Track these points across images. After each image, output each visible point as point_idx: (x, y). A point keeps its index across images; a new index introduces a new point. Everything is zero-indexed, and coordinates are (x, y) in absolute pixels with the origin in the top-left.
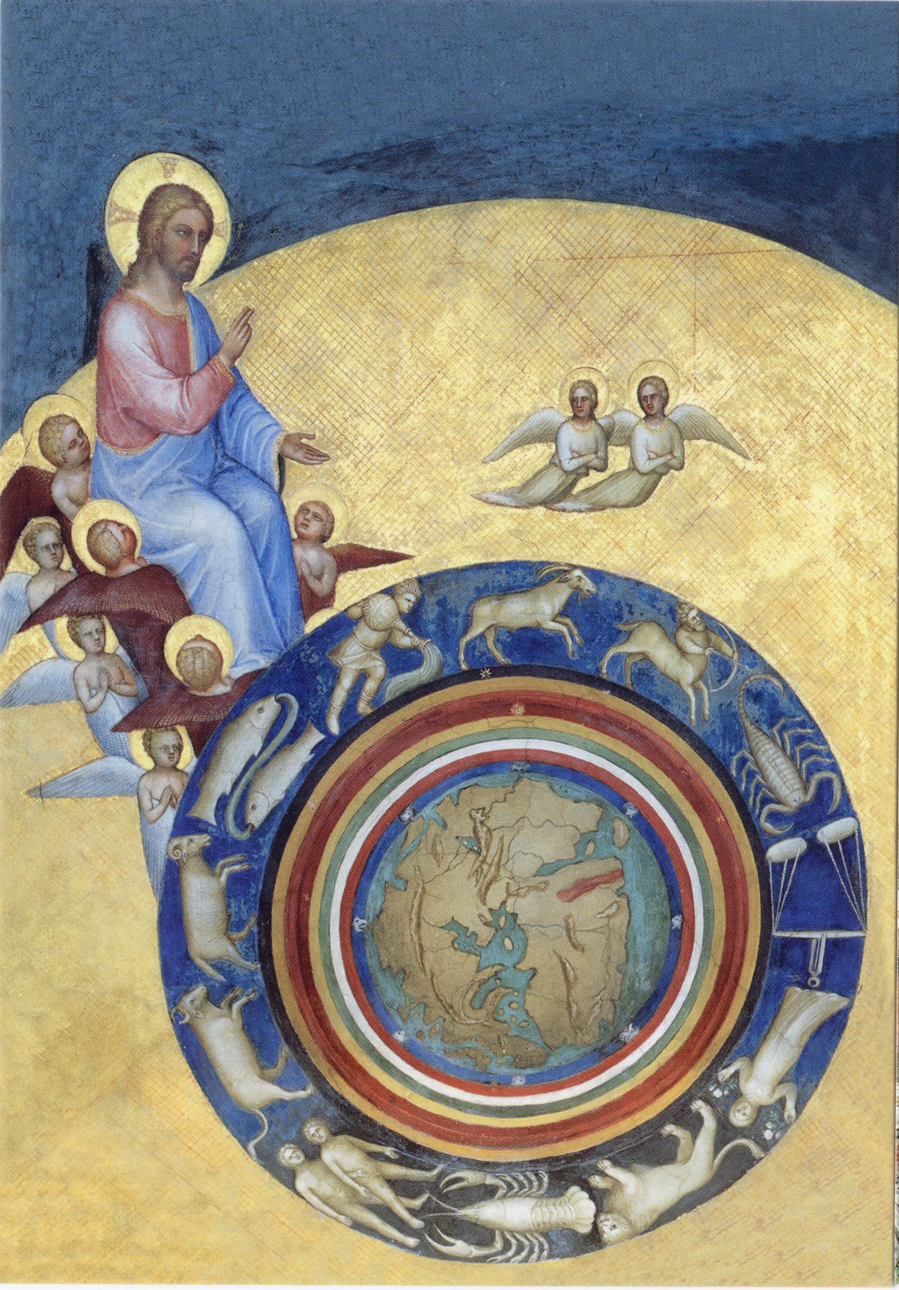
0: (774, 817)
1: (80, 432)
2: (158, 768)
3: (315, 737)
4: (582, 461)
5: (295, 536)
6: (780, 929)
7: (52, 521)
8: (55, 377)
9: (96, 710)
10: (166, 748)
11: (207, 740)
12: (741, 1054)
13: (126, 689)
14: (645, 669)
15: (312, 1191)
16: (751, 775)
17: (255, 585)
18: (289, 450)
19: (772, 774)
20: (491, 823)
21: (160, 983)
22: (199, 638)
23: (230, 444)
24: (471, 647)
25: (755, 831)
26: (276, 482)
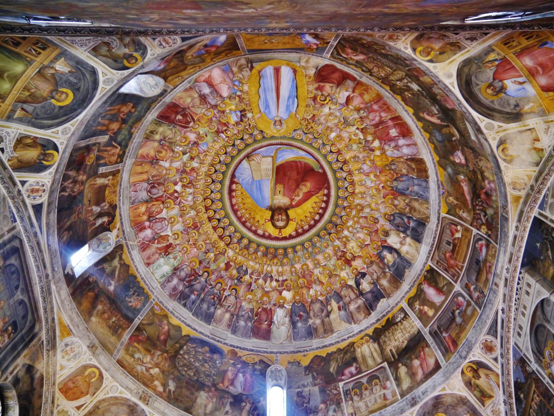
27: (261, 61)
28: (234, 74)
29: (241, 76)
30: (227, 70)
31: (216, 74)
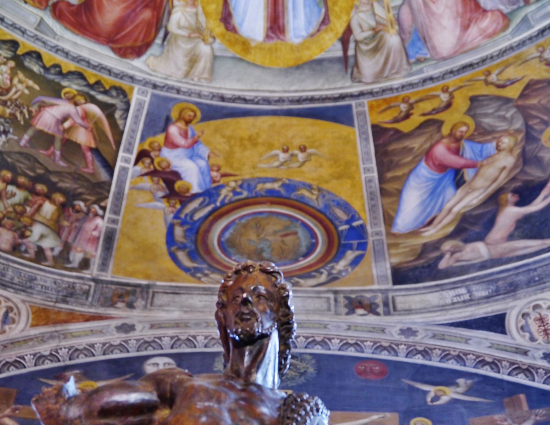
6: (344, 240)
8: (155, 134)
11: (184, 204)
14: (303, 197)
27: (320, 62)
28: (398, 21)
29: (379, 10)
30: (417, 39)
31: (445, 34)
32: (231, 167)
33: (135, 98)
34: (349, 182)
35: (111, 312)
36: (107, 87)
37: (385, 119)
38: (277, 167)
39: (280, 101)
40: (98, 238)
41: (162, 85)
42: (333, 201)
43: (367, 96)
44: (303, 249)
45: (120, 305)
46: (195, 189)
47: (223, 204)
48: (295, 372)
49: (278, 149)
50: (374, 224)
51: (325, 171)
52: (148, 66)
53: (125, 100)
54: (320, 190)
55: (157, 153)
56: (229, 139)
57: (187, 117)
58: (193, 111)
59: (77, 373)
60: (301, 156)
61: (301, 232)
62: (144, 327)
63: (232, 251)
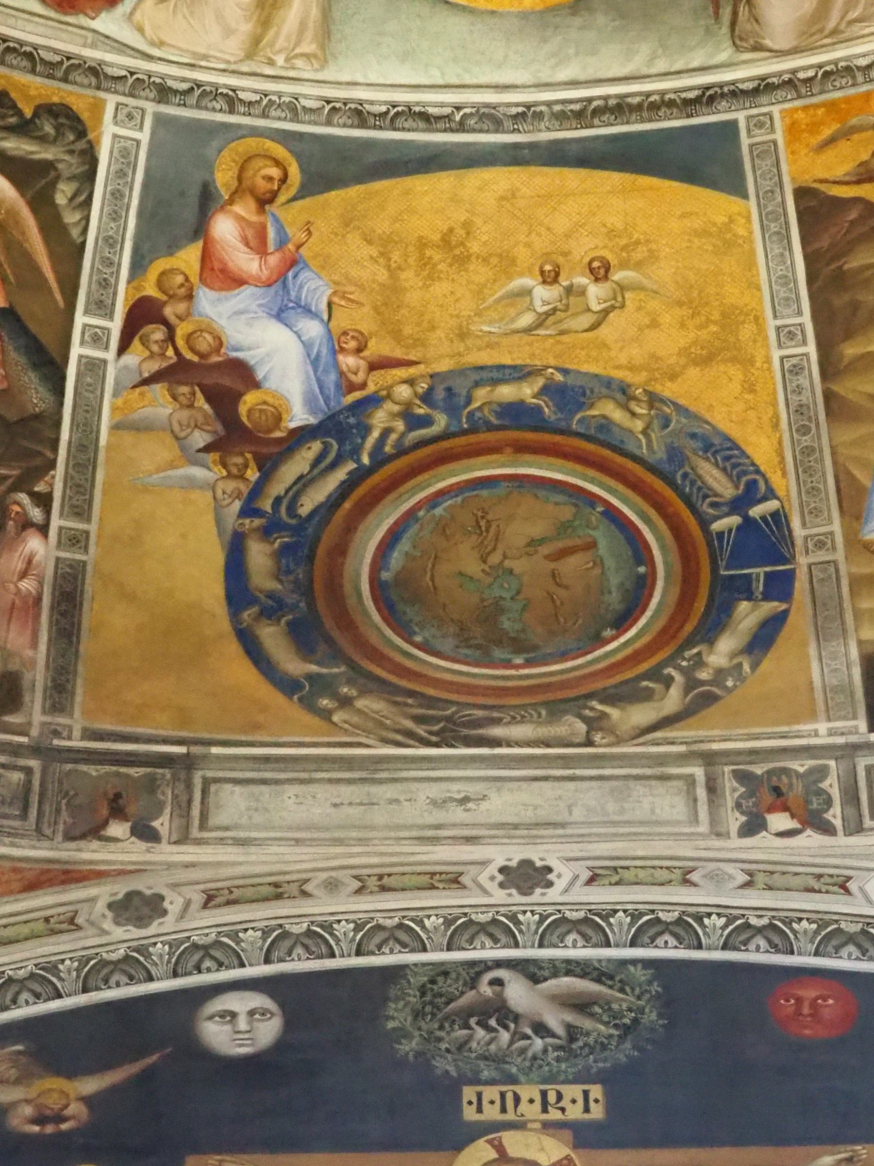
0: (714, 505)
1: (187, 279)
2: (230, 476)
3: (351, 466)
4: (550, 307)
5: (337, 347)
6: (727, 568)
7: (162, 327)
9: (185, 438)
10: (236, 465)
11: (268, 466)
12: (702, 641)
13: (209, 428)
14: (606, 424)
15: (346, 722)
16: (693, 483)
17: (308, 377)
18: (336, 299)
19: (710, 481)
20: (489, 517)
21: (224, 603)
22: (265, 403)
23: (293, 294)
24: (471, 414)
25: (700, 515)
26: (326, 317)
32: (397, 335)
33: (108, 136)
34: (736, 372)
35: (90, 853)
36: (28, 113)
37: (833, 168)
38: (528, 330)
39: (527, 115)
40: (38, 600)
41: (185, 86)
42: (693, 436)
43: (780, 94)
44: (614, 600)
45: (118, 829)
46: (299, 416)
47: (380, 460)
48: (606, 1024)
49: (530, 271)
50: (811, 513)
51: (669, 342)
52: (141, 30)
53: (81, 145)
54: (653, 399)
55: (181, 307)
56: (385, 245)
57: (262, 185)
58: (277, 163)
59: (19, 1053)
60: (596, 294)
61: (605, 539)
62: (188, 904)
63: (411, 613)
